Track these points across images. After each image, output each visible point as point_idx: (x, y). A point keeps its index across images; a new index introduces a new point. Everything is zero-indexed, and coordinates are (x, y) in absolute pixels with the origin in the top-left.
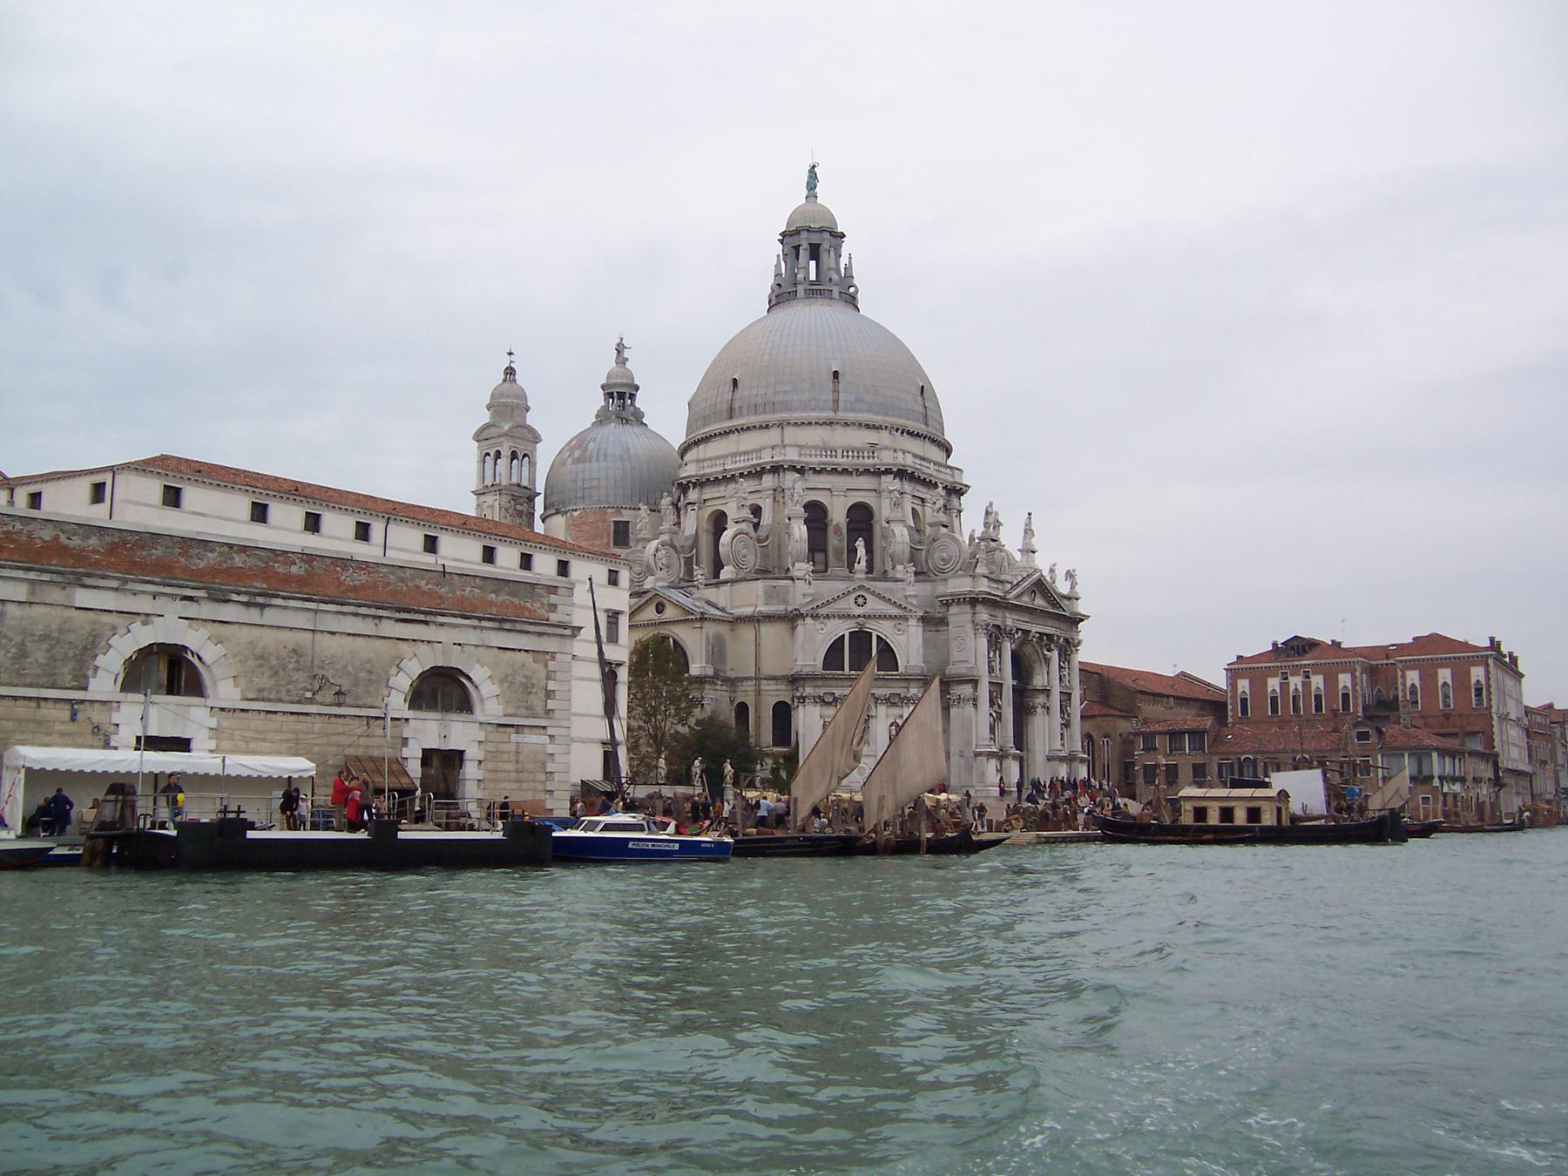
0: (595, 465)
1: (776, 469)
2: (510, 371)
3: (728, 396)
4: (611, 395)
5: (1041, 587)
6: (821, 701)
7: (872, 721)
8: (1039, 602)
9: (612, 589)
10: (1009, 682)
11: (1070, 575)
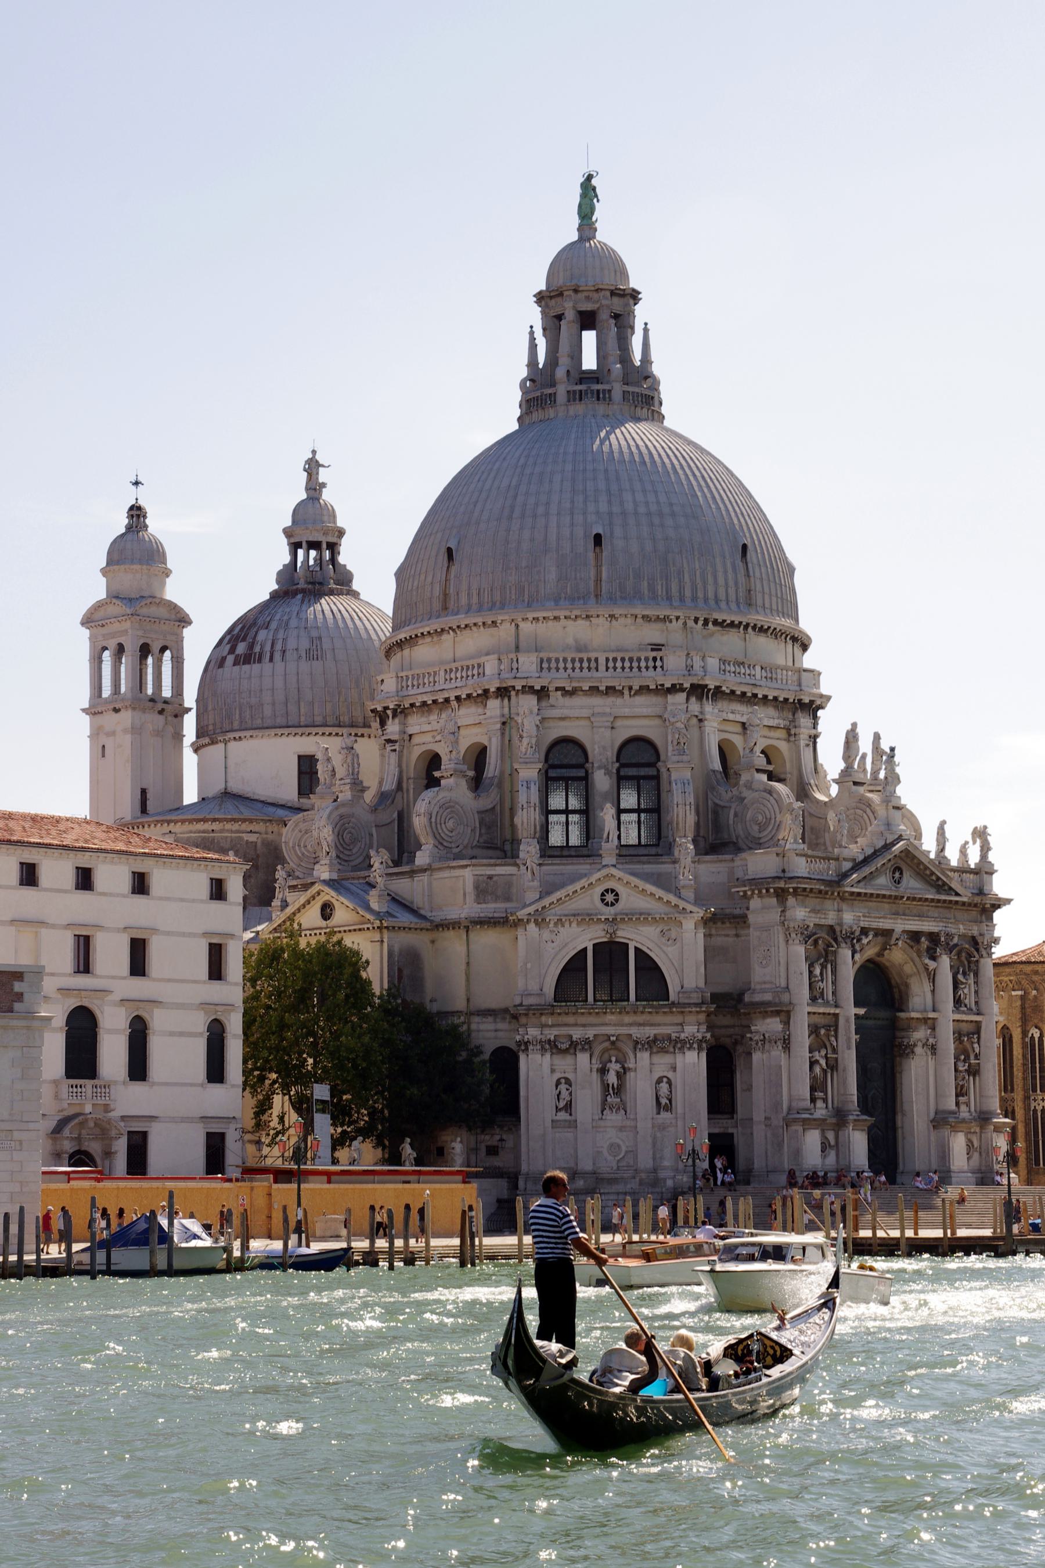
0: (267, 666)
1: (503, 692)
2: (136, 513)
3: (440, 575)
4: (295, 546)
5: (910, 861)
6: (552, 1047)
7: (630, 1075)
8: (911, 884)
9: (217, 905)
10: (850, 1011)
11: (981, 834)
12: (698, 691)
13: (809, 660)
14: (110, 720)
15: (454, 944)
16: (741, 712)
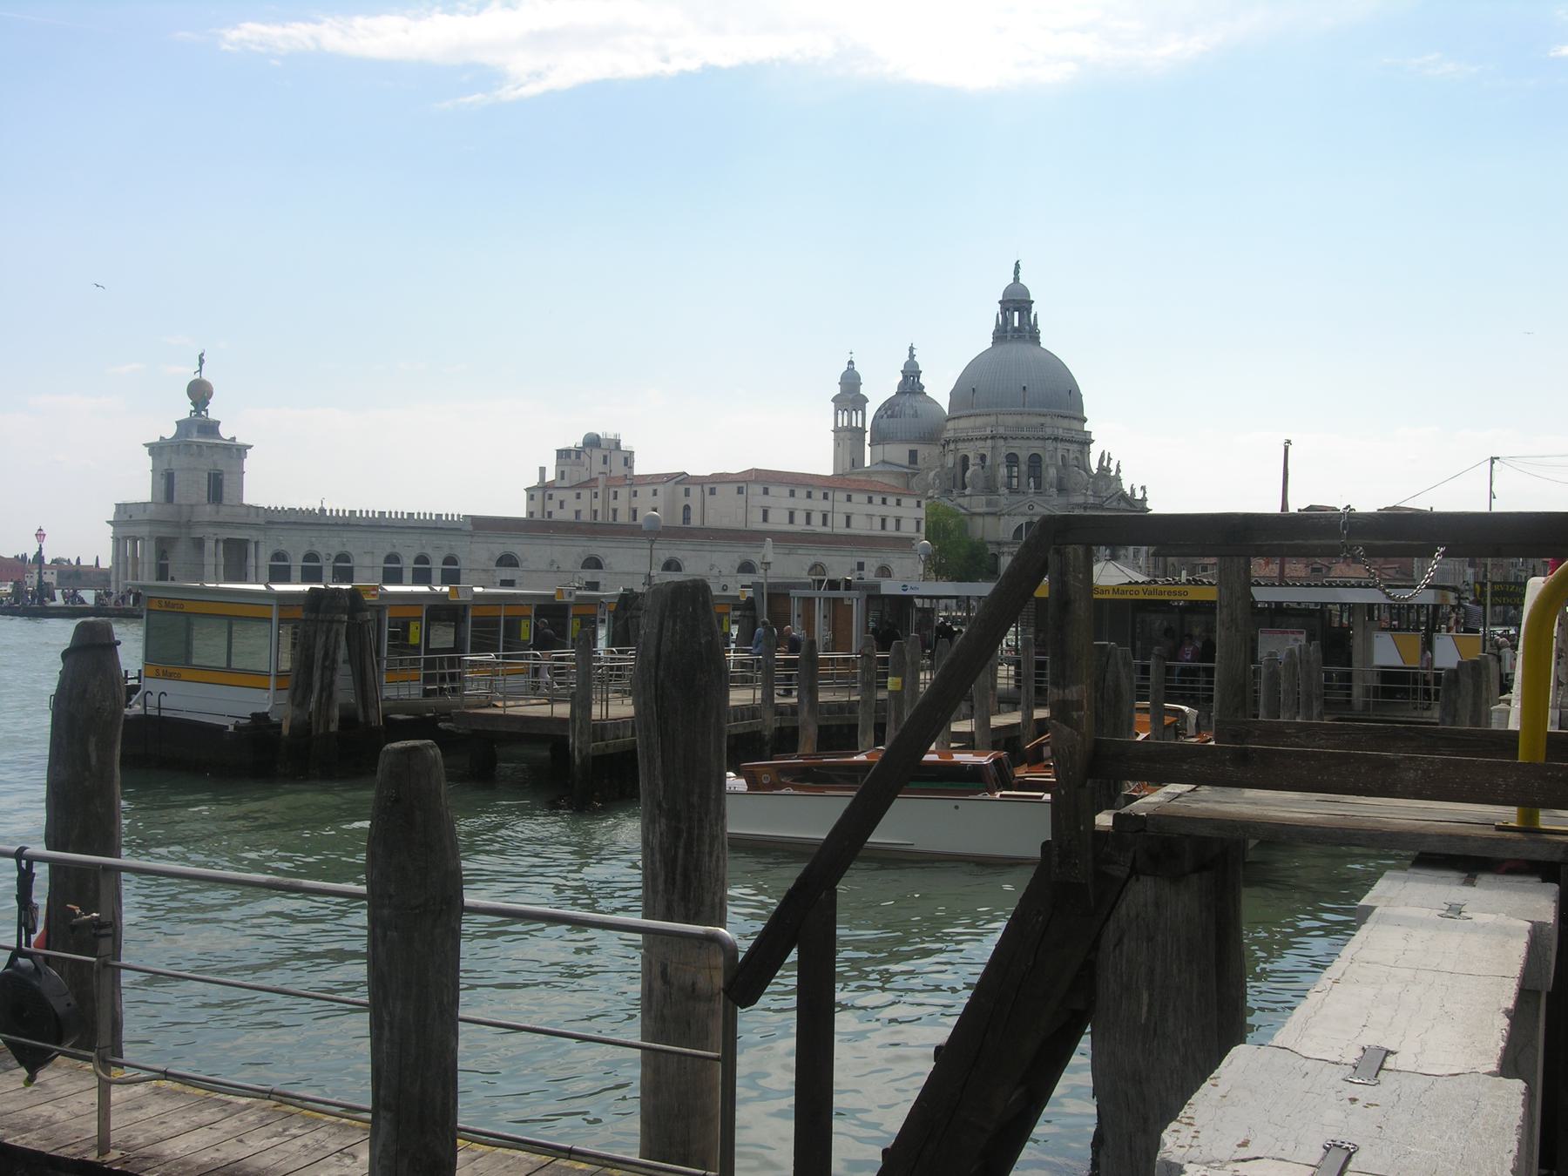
1: (993, 438)
2: (851, 362)
5: (1123, 496)
8: (1123, 505)
11: (1143, 488)
12: (1056, 439)
13: (1087, 427)
14: (842, 435)
15: (979, 521)
16: (1068, 446)
